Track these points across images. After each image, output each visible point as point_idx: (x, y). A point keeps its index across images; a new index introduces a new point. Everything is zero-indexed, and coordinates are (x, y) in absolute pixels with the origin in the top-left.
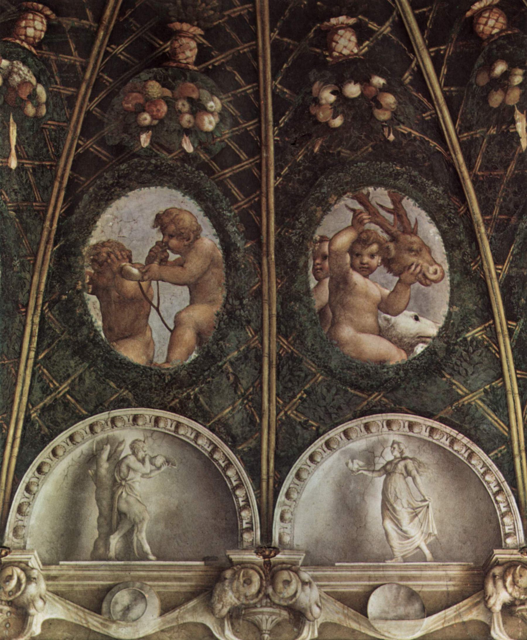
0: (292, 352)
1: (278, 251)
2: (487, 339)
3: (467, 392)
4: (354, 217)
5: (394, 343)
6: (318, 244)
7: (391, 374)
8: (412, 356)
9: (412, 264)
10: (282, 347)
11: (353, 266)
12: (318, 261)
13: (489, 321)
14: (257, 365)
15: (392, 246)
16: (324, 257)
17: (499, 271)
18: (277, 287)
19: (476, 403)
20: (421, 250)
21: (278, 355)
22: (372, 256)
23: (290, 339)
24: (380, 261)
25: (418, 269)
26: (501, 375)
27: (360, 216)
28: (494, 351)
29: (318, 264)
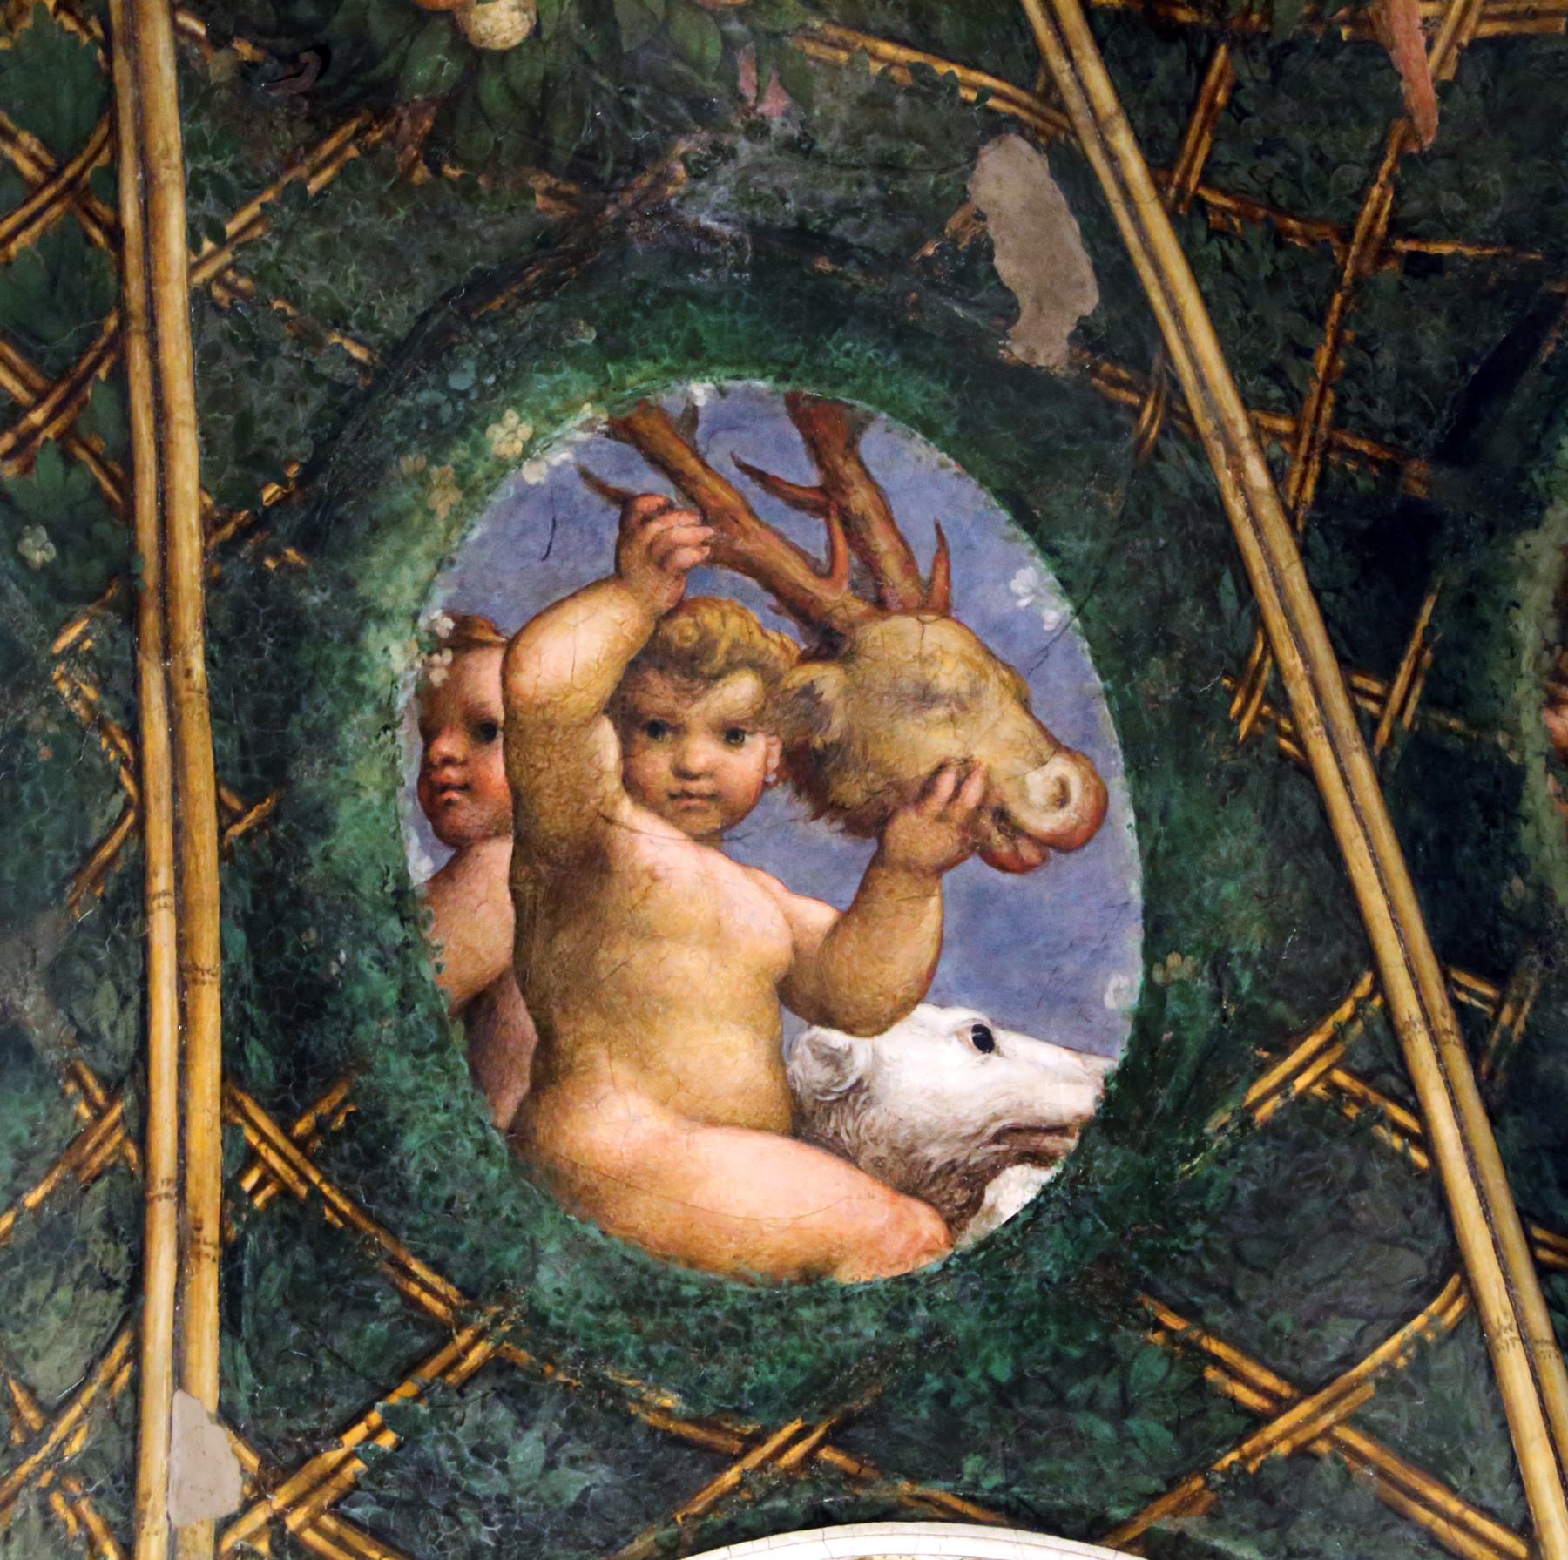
0: (315, 1192)
1: (223, 641)
2: (1357, 1088)
3: (1285, 1391)
4: (627, 534)
5: (878, 1169)
6: (448, 656)
7: (869, 1327)
8: (976, 1230)
9: (941, 768)
10: (251, 1157)
11: (632, 784)
12: (448, 745)
13: (1355, 981)
14: (114, 1260)
15: (828, 679)
16: (483, 730)
17: (1372, 707)
18: (222, 831)
19: (1336, 1441)
20: (975, 693)
21: (230, 1189)
22: (732, 735)
23: (301, 1128)
24: (774, 762)
25: (972, 793)
26: (1454, 1260)
27: (655, 528)
28: (1397, 1143)
29: (448, 761)
